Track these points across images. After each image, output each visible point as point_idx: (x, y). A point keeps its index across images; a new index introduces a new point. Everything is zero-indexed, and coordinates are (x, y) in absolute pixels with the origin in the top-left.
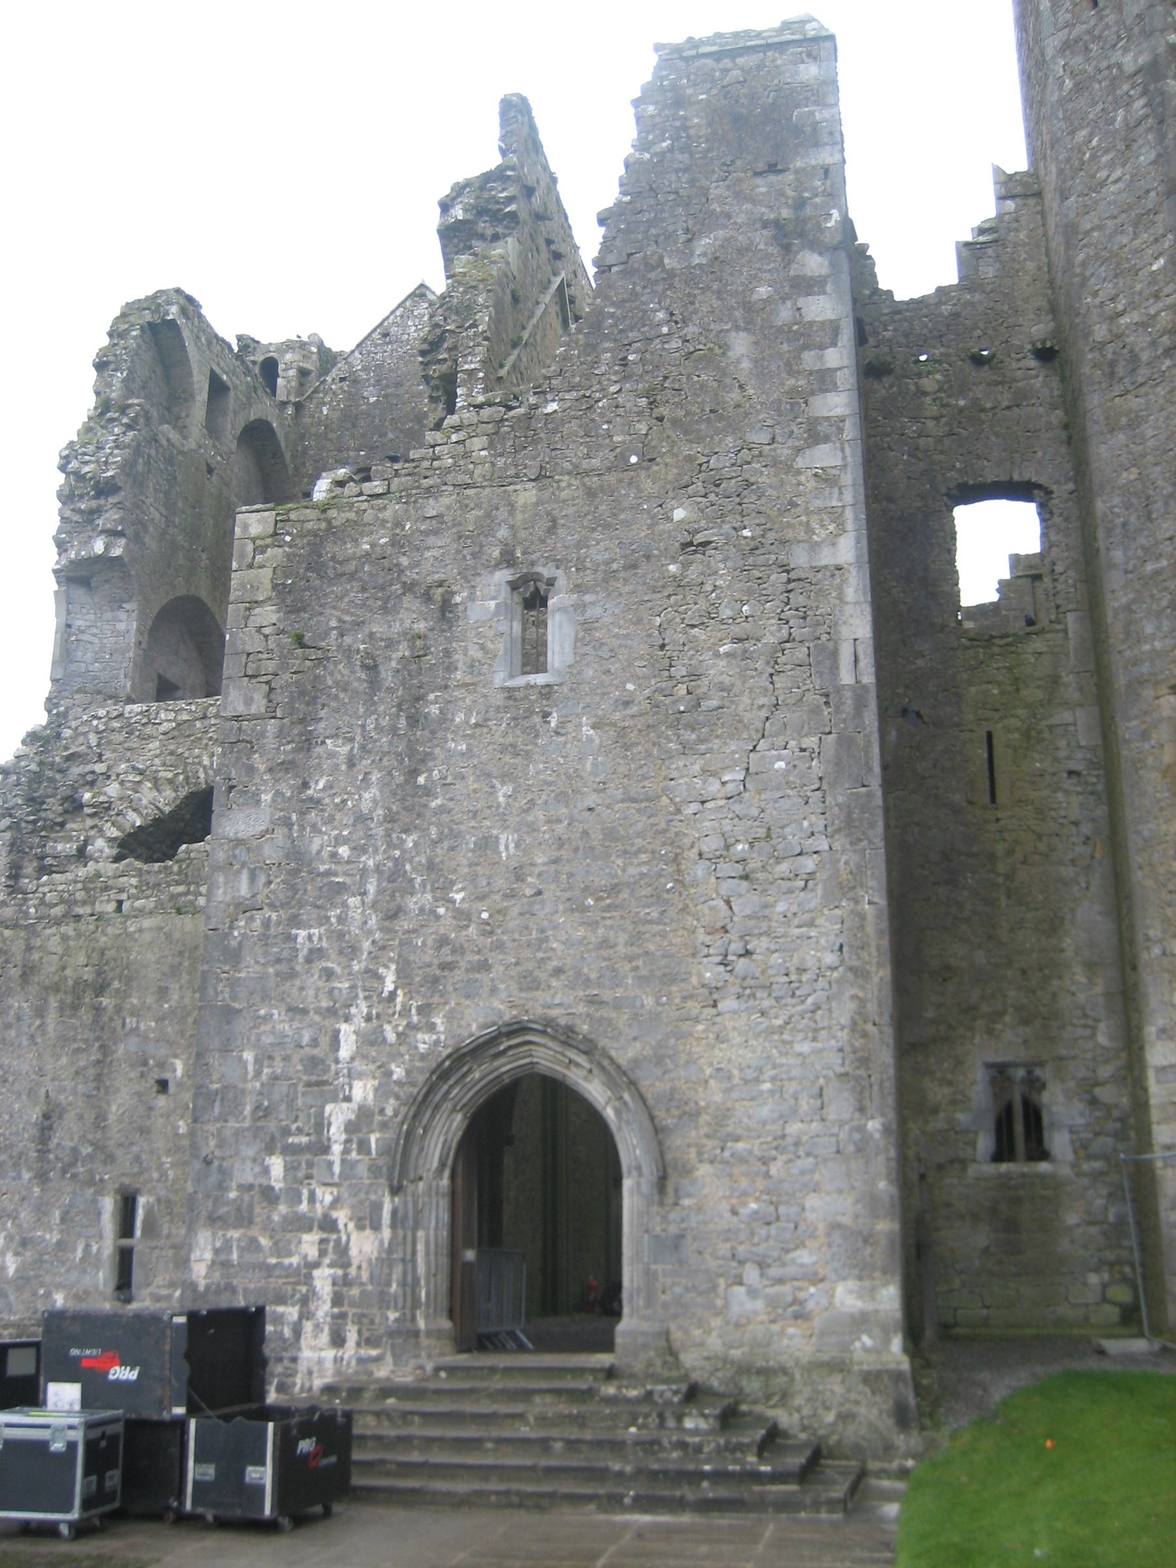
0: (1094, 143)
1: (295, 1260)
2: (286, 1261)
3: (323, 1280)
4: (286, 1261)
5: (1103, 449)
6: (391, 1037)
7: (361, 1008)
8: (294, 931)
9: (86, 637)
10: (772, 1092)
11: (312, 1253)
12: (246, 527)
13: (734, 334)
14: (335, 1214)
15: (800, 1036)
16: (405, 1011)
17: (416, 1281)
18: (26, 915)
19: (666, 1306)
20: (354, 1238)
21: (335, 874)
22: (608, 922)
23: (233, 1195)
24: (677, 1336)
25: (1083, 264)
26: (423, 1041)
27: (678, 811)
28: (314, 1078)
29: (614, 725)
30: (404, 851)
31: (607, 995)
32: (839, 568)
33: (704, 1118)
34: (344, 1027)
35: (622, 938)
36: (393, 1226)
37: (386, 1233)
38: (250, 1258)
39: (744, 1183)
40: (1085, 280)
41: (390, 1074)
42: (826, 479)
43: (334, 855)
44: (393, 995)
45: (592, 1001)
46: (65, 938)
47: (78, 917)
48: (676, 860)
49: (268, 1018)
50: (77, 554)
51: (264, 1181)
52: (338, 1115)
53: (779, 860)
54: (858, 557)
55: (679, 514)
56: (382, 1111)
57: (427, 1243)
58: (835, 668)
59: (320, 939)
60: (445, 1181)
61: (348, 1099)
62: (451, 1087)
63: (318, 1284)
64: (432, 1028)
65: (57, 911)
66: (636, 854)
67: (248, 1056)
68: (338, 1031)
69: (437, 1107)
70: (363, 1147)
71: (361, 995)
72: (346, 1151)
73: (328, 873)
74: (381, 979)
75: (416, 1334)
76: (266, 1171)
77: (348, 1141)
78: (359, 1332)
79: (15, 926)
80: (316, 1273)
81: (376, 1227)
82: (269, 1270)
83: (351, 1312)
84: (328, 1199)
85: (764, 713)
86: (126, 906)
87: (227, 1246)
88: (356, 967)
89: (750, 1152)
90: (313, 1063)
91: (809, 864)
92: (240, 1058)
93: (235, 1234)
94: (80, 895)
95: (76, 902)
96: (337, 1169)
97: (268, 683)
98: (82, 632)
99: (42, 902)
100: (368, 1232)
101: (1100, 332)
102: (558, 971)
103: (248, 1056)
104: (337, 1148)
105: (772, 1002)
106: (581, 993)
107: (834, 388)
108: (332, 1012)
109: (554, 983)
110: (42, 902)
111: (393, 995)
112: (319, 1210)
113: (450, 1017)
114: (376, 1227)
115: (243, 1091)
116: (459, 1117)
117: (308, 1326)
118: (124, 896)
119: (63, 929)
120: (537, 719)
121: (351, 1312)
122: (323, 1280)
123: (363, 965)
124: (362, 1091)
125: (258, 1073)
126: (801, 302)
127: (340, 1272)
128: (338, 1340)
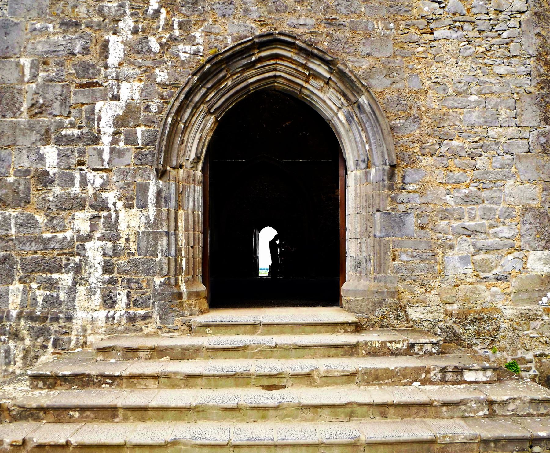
1: (69, 234)
2: (60, 236)
7: (127, 23)
10: (478, 103)
11: (85, 228)
14: (104, 195)
15: (499, 61)
16: (169, 26)
19: (396, 270)
20: (122, 215)
23: (11, 179)
24: (405, 295)
28: (85, 81)
34: (112, 38)
36: (158, 204)
37: (152, 210)
38: (28, 233)
39: (457, 174)
44: (157, 12)
49: (43, 31)
51: (40, 167)
57: (187, 220)
60: (199, 173)
62: (209, 90)
63: (90, 254)
64: (192, 40)
67: (26, 62)
68: (108, 41)
69: (196, 107)
70: (131, 140)
71: (128, 12)
72: (114, 142)
75: (180, 295)
76: (41, 158)
77: (116, 133)
78: (129, 297)
80: (88, 245)
81: (143, 206)
84: (99, 182)
89: (462, 148)
90: (86, 68)
96: (106, 156)
100: (135, 209)
103: (26, 62)
104: (106, 139)
105: (477, 34)
108: (99, 27)
111: (157, 12)
113: (208, 33)
114: (143, 206)
115: (20, 91)
116: (212, 119)
117: (81, 290)
125: (34, 76)
127: (110, 244)
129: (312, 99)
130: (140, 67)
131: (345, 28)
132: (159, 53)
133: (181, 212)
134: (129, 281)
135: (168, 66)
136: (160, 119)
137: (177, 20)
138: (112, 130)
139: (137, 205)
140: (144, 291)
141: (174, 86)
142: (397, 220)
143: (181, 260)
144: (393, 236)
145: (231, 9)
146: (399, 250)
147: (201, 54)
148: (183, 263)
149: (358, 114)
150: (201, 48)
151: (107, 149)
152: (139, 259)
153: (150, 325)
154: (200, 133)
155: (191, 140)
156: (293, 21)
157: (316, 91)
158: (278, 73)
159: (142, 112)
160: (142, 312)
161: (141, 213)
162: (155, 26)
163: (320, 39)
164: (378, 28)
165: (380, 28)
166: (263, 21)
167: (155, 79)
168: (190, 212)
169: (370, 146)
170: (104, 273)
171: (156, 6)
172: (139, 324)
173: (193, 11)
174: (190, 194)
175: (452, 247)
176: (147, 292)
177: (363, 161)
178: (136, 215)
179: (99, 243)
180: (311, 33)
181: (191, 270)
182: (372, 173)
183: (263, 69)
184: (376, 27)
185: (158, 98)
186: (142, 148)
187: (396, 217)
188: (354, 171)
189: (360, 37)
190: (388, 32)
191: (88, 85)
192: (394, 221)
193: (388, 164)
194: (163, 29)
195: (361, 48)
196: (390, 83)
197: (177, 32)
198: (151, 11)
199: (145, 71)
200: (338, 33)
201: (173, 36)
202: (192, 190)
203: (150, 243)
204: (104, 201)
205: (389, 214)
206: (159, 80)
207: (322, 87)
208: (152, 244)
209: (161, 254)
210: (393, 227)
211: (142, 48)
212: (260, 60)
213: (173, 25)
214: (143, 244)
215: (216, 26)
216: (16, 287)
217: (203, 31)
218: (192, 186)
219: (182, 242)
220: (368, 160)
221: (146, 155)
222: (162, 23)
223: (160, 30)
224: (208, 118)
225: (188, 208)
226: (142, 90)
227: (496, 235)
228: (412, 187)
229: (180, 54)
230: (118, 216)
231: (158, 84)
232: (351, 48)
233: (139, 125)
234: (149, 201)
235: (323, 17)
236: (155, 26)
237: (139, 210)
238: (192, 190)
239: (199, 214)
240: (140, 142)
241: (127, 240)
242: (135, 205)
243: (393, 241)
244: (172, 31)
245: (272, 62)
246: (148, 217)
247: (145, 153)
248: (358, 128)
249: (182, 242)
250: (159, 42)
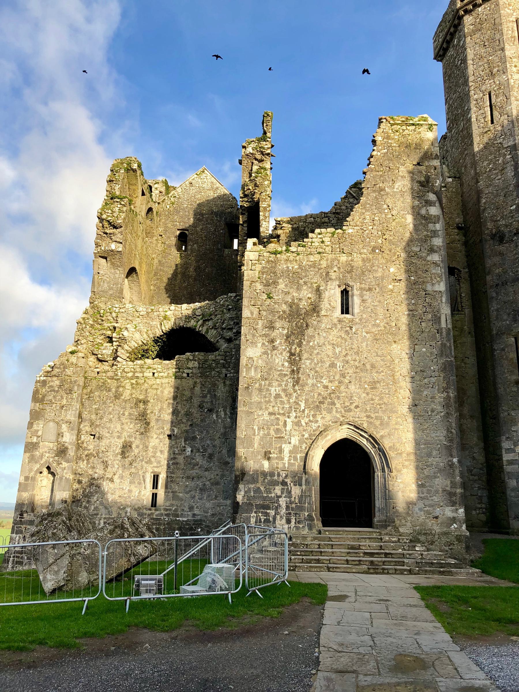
0: (491, 166)
1: (273, 495)
2: (270, 495)
3: (283, 502)
4: (270, 495)
5: (489, 261)
6: (304, 424)
7: (293, 414)
8: (270, 388)
9: (105, 278)
11: (279, 493)
12: (248, 256)
13: (407, 215)
14: (286, 480)
16: (308, 416)
18: (117, 375)
21: (283, 371)
22: (372, 393)
25: (485, 203)
26: (314, 426)
27: (393, 361)
29: (373, 332)
30: (306, 366)
31: (373, 415)
32: (440, 292)
33: (404, 455)
34: (288, 420)
35: (378, 398)
40: (485, 209)
41: (303, 435)
42: (435, 264)
43: (283, 365)
44: (304, 411)
45: (368, 417)
46: (132, 384)
47: (137, 377)
48: (393, 375)
50: (105, 248)
52: (287, 448)
53: (425, 378)
54: (446, 289)
55: (392, 270)
56: (301, 447)
58: (440, 322)
59: (279, 391)
61: (290, 443)
63: (281, 503)
65: (130, 375)
66: (380, 373)
67: (256, 428)
70: (295, 459)
71: (293, 410)
72: (289, 460)
73: (281, 370)
74: (300, 405)
79: (112, 378)
80: (280, 499)
81: (300, 485)
82: (264, 498)
84: (284, 475)
85: (419, 334)
86: (156, 375)
87: (249, 489)
88: (291, 401)
90: (278, 431)
91: (433, 380)
92: (253, 428)
93: (252, 486)
94: (138, 370)
95: (137, 372)
96: (287, 465)
97: (259, 308)
98: (103, 276)
99: (123, 370)
100: (298, 486)
101: (490, 225)
102: (357, 407)
103: (256, 428)
104: (286, 459)
107: (438, 236)
109: (356, 410)
110: (123, 370)
111: (304, 411)
112: (281, 479)
114: (300, 485)
117: (278, 517)
118: (155, 371)
119: (132, 381)
120: (348, 329)
121: (292, 512)
122: (283, 502)
123: (293, 401)
124: (295, 441)
126: (428, 208)
128: (288, 521)
134: (296, 514)
138: (289, 455)
151: (287, 462)
170: (286, 510)
179: (284, 499)
191: (279, 437)
198: (301, 410)
216: (253, 514)
227: (432, 500)
230: (291, 488)
241: (295, 498)
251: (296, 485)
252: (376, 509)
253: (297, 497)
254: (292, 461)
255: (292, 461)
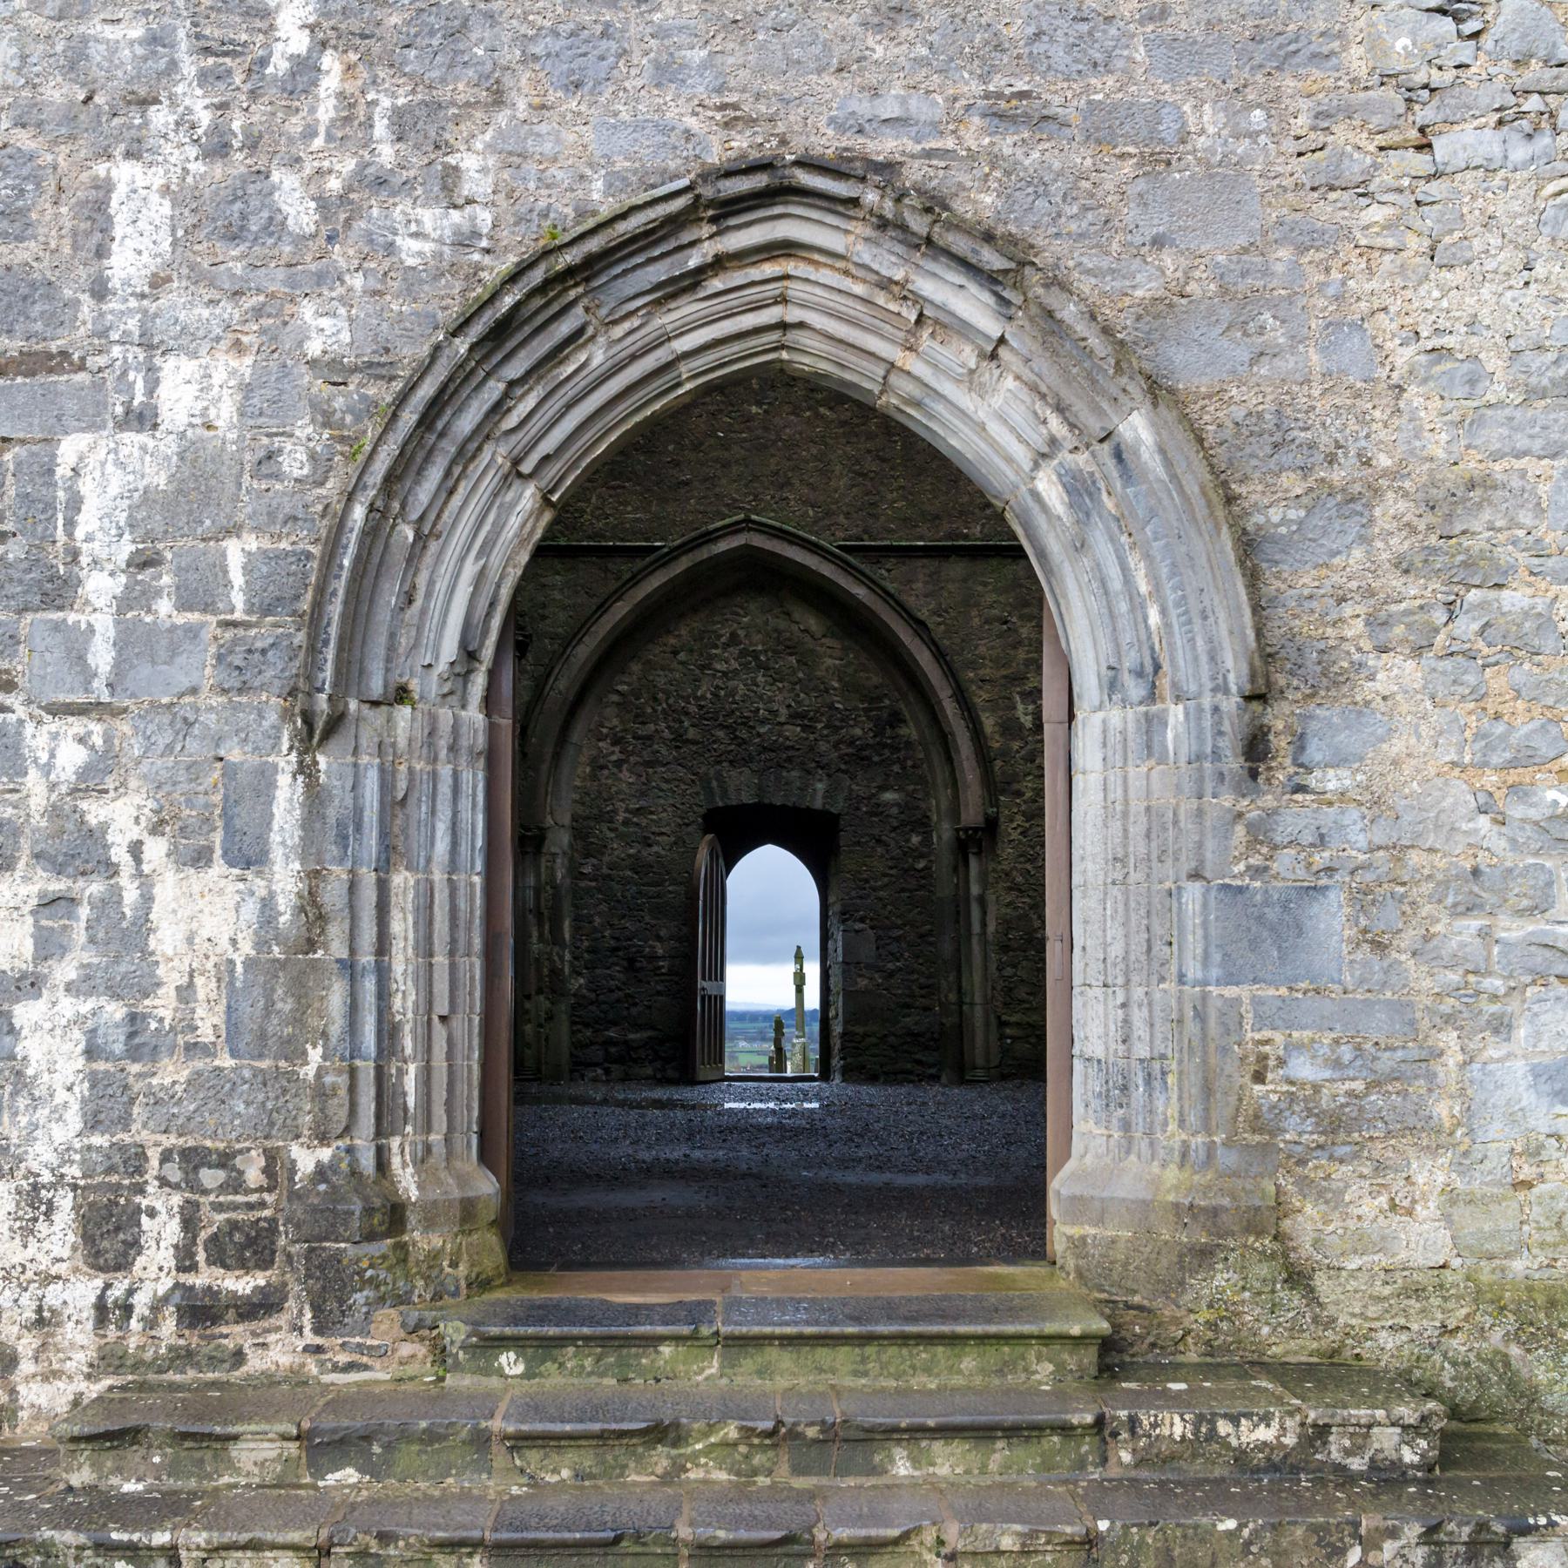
6: (300, 213)
14: (95, 811)
17: (388, 1033)
33: (1391, 507)
34: (124, 173)
36: (309, 847)
37: (285, 879)
44: (305, 70)
60: (474, 715)
61: (143, 419)
68: (105, 187)
69: (465, 455)
71: (189, 66)
72: (132, 600)
77: (144, 562)
78: (190, 1223)
83: (154, 1142)
84: (71, 758)
96: (102, 657)
100: (219, 867)
104: (101, 587)
106: (976, 88)
111: (305, 70)
113: (513, 158)
116: (527, 497)
127: (115, 1011)
129: (931, 417)
130: (237, 293)
131: (1067, 131)
132: (314, 236)
133: (401, 879)
135: (350, 289)
136: (320, 508)
137: (386, 102)
138: (126, 549)
139: (225, 854)
140: (253, 1198)
141: (375, 370)
142: (1272, 914)
143: (401, 1073)
144: (1255, 981)
145: (602, 58)
146: (1279, 1038)
147: (484, 243)
148: (410, 1083)
149: (1118, 484)
150: (485, 218)
151: (104, 624)
152: (234, 1070)
153: (272, 1338)
154: (478, 558)
155: (441, 586)
156: (854, 105)
157: (947, 388)
158: (793, 314)
159: (247, 477)
160: (242, 1284)
161: (241, 886)
162: (295, 125)
163: (965, 179)
164: (1203, 132)
165: (1211, 130)
166: (735, 107)
167: (300, 344)
168: (438, 876)
169: (1163, 612)
170: (93, 1123)
171: (300, 43)
172: (235, 1334)
173: (450, 66)
174: (439, 807)
175: (1501, 1027)
176: (262, 1205)
177: (1139, 673)
178: (221, 892)
179: (68, 1006)
180: (929, 154)
181: (439, 1112)
182: (1171, 721)
183: (732, 300)
184: (1191, 120)
185: (313, 421)
186: (246, 625)
187: (1267, 903)
188: (1100, 708)
189: (1128, 168)
190: (1243, 147)
192: (1260, 919)
193: (1234, 689)
194: (330, 138)
195: (1130, 214)
196: (1246, 357)
197: (387, 154)
198: (279, 65)
199: (258, 312)
200: (1036, 155)
201: (371, 170)
202: (445, 789)
203: (279, 1005)
204: (95, 836)
205: (1240, 890)
206: (314, 348)
207: (972, 372)
208: (288, 1007)
209: (320, 1050)
210: (1254, 945)
211: (243, 216)
212: (719, 263)
213: (369, 124)
214: (249, 1012)
215: (543, 128)
217: (490, 147)
218: (445, 771)
219: (405, 1002)
220: (1157, 667)
221: (264, 652)
222: (326, 111)
223: (319, 142)
224: (510, 496)
225: (429, 860)
226: (247, 389)
228: (1333, 781)
229: (399, 241)
230: (147, 899)
231: (313, 363)
232: (1090, 216)
233: (234, 530)
234: (275, 838)
235: (976, 88)
236: (295, 125)
237: (236, 871)
238: (445, 789)
239: (472, 885)
240: (238, 599)
241: (186, 993)
242: (218, 852)
243: (1257, 1002)
244: (365, 146)
245: (769, 269)
246: (268, 903)
247: (259, 645)
248: (1112, 540)
249: (405, 1002)
250: (313, 190)
251: (201, 858)
252: (1084, 1087)
253: (205, 987)
254: (164, 606)
255: (164, 606)
